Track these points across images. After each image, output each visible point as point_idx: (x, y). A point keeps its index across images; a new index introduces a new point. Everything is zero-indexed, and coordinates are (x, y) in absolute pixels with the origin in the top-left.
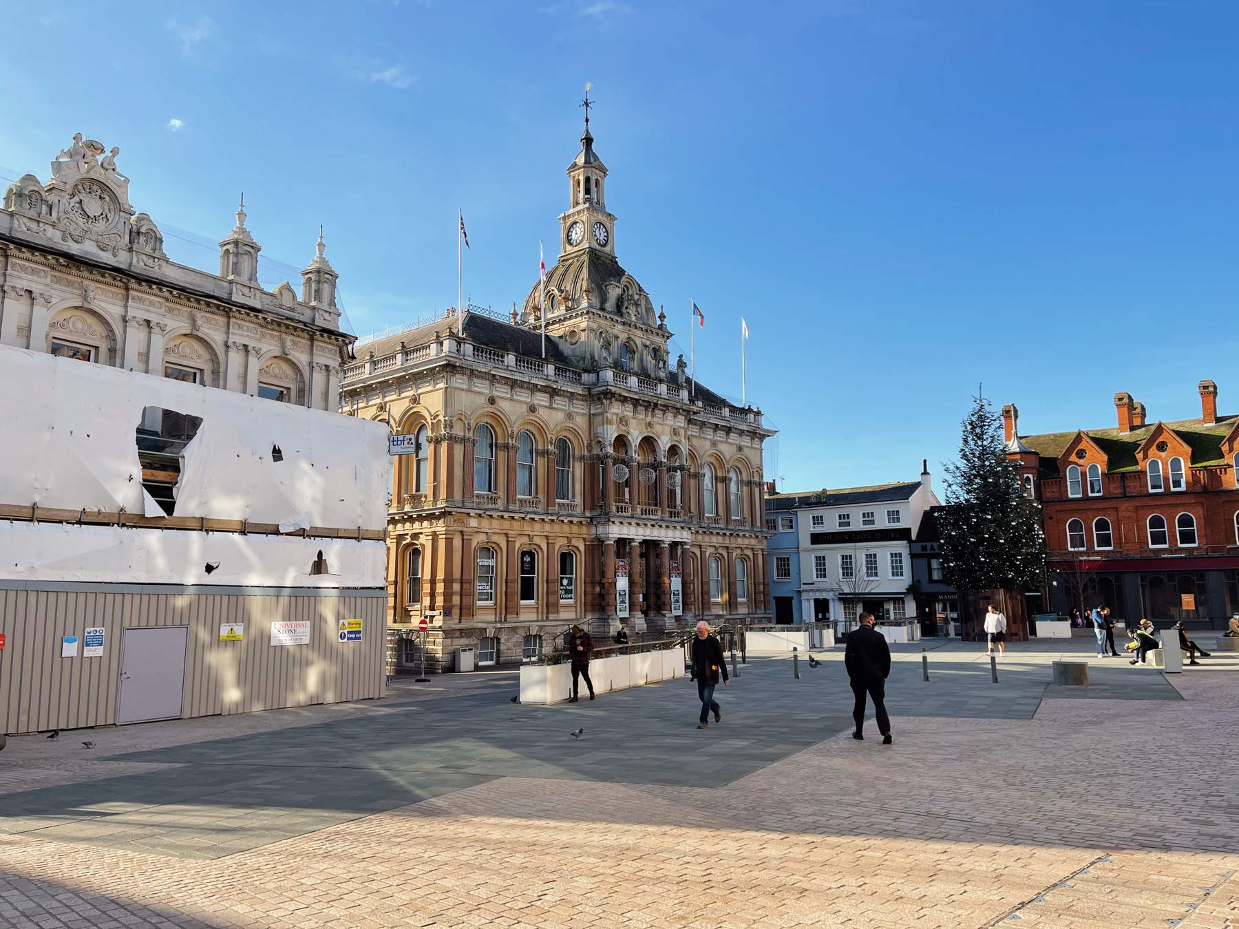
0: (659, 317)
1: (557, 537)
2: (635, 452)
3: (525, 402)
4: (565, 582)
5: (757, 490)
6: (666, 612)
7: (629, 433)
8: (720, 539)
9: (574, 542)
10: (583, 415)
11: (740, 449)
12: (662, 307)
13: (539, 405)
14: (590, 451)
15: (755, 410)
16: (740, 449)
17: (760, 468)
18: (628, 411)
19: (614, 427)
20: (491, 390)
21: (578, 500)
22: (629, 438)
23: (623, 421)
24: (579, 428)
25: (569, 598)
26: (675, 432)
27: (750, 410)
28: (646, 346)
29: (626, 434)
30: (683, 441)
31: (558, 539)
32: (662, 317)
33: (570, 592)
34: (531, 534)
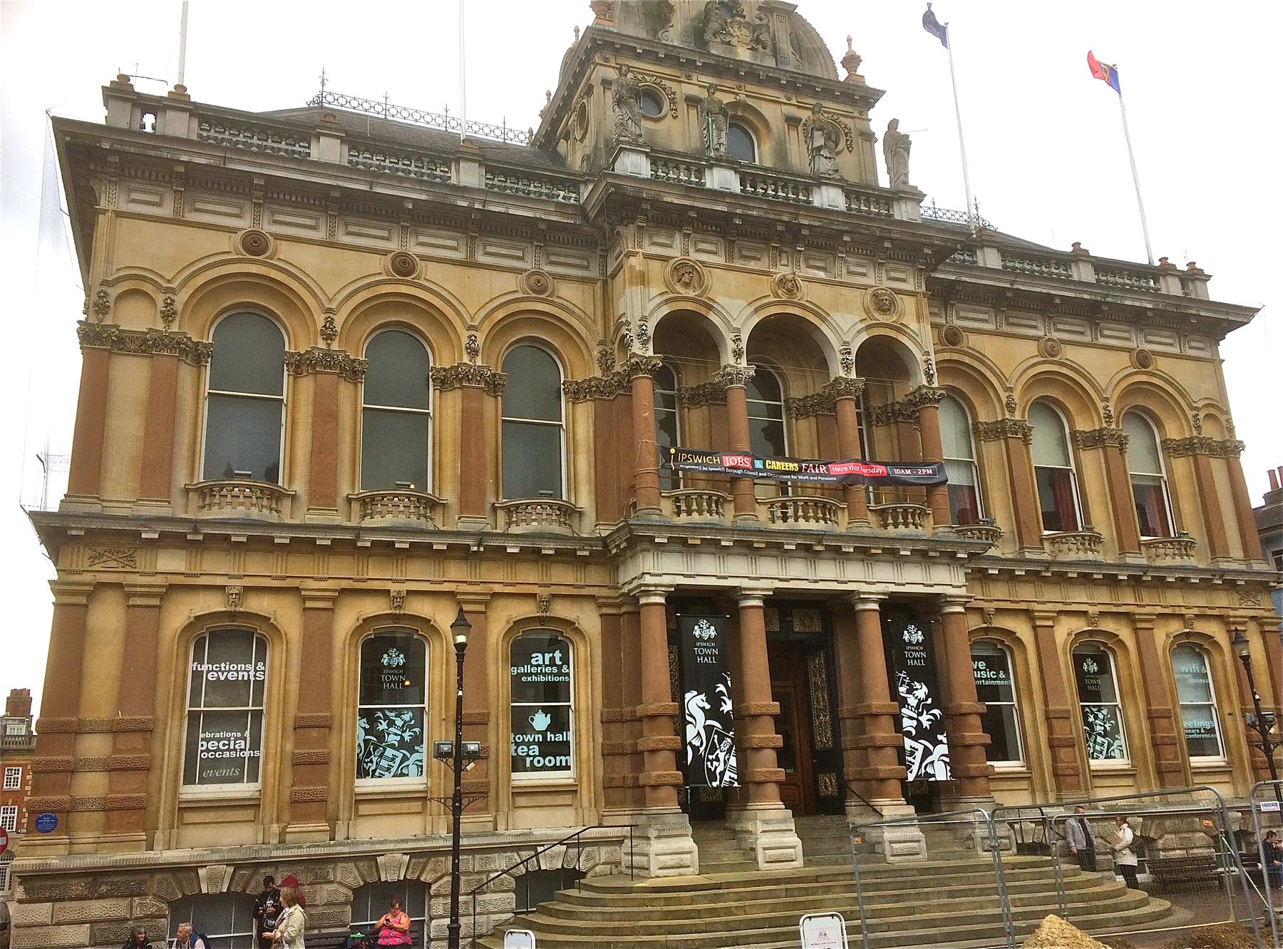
0: (845, 63)
1: (495, 595)
2: (738, 354)
3: (384, 253)
4: (541, 721)
5: (1217, 467)
6: (886, 801)
7: (710, 308)
8: (1103, 596)
9: (562, 610)
10: (583, 280)
11: (1143, 360)
12: (849, 40)
13: (424, 258)
14: (606, 365)
15: (1182, 267)
16: (1143, 360)
17: (1218, 410)
18: (708, 254)
19: (654, 291)
20: (256, 219)
21: (585, 500)
22: (713, 317)
23: (685, 272)
24: (572, 313)
25: (555, 768)
26: (883, 303)
27: (1166, 269)
28: (792, 122)
29: (703, 311)
30: (914, 325)
31: (501, 604)
32: (852, 61)
33: (563, 748)
34: (394, 587)
